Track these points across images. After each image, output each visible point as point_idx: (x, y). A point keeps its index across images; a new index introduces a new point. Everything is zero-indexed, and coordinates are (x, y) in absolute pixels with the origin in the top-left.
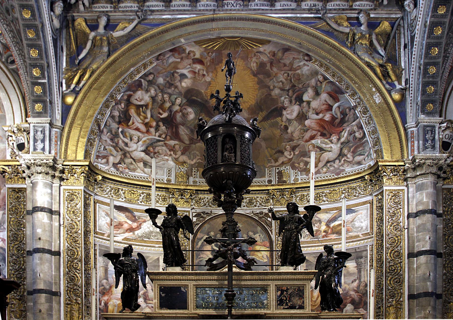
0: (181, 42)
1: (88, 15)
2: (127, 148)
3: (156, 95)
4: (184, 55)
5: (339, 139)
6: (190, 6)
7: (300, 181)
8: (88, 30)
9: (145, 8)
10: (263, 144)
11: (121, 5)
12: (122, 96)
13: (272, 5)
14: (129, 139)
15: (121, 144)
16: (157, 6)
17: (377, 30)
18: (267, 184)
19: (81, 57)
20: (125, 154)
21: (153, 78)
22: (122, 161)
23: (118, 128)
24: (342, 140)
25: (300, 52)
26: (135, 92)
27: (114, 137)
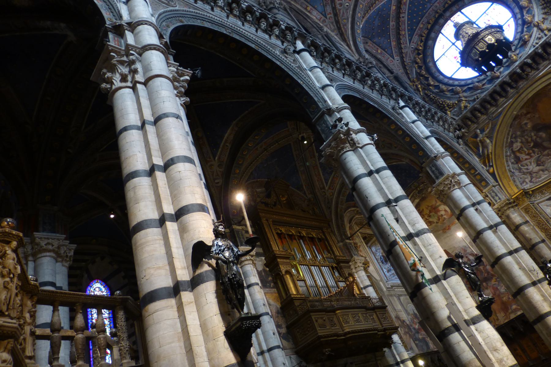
2: (529, 171)
8: (475, 140)
20: (530, 173)
26: (512, 146)
27: (520, 170)
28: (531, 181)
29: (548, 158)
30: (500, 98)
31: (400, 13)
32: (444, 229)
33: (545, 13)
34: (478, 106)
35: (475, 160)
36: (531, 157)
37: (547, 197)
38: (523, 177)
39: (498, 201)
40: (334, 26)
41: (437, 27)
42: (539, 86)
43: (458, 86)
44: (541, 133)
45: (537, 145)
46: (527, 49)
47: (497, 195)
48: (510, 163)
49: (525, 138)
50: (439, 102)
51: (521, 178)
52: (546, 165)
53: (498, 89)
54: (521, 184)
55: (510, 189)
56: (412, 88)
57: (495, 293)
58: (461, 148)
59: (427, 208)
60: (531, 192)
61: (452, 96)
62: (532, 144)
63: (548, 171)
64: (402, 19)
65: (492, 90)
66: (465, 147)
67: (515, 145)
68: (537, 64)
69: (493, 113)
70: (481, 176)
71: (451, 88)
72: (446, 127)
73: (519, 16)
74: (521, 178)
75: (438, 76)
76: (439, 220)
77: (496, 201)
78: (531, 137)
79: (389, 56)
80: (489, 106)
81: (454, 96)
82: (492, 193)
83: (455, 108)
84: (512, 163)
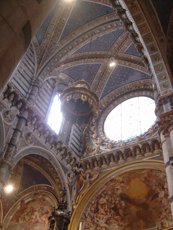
0: (113, 177)
1: (84, 175)
2: (98, 223)
4: (116, 181)
6: (116, 164)
8: (84, 180)
9: (102, 168)
12: (95, 202)
14: (99, 218)
15: (96, 221)
16: (105, 166)
19: (81, 190)
20: (97, 225)
21: (106, 192)
23: (94, 215)
25: (156, 170)
26: (100, 199)
29: (115, 222)
36: (107, 214)
38: (91, 225)
40: (41, 52)
41: (121, 99)
44: (122, 202)
45: (115, 209)
48: (89, 209)
49: (111, 199)
52: (110, 226)
59: (30, 208)
62: (113, 206)
64: (104, 82)
67: (102, 200)
68: (145, 152)
74: (88, 225)
75: (100, 128)
76: (29, 220)
78: (116, 201)
84: (91, 211)
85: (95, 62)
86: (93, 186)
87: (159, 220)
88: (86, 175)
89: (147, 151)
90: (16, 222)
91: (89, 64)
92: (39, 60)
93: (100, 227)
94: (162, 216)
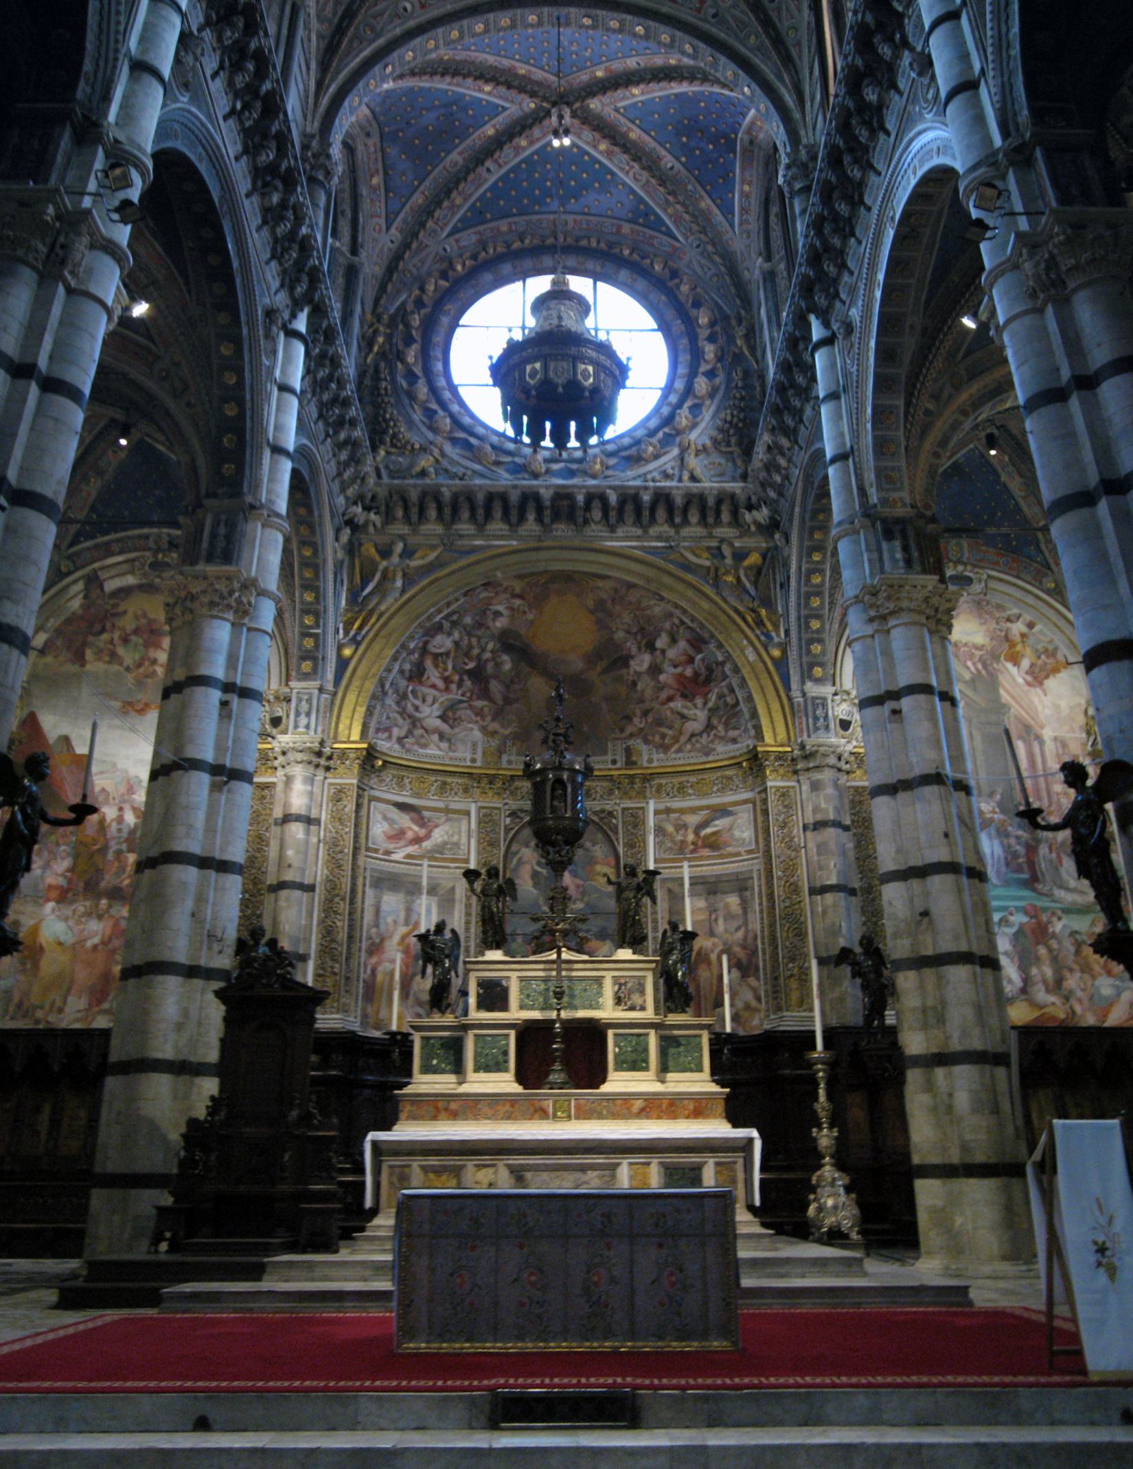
2: (417, 715)
3: (461, 639)
4: (499, 589)
5: (705, 704)
7: (655, 764)
8: (377, 558)
10: (604, 705)
11: (423, 527)
13: (613, 531)
15: (410, 708)
17: (746, 563)
18: (610, 766)
20: (415, 722)
22: (409, 733)
24: (710, 705)
25: (648, 590)
26: (433, 637)
28: (400, 740)
30: (502, 519)
31: (492, 156)
32: (130, 704)
33: (715, 442)
34: (447, 494)
35: (336, 602)
36: (447, 689)
37: (400, 799)
38: (395, 719)
39: (301, 729)
42: (582, 563)
43: (452, 416)
46: (630, 473)
47: (308, 714)
48: (397, 667)
50: (385, 412)
51: (388, 718)
52: (457, 730)
53: (514, 497)
54: (378, 730)
55: (348, 722)
56: (362, 326)
57: (110, 940)
58: (332, 549)
60: (380, 763)
61: (420, 425)
63: (450, 748)
65: (502, 490)
66: (340, 555)
67: (439, 639)
68: (621, 519)
69: (461, 536)
70: (317, 646)
71: (434, 406)
72: (347, 475)
73: (673, 399)
74: (388, 718)
76: (139, 665)
77: (296, 727)
79: (383, 212)
80: (465, 514)
81: (424, 429)
82: (304, 703)
83: (402, 454)
84: (401, 672)
85: (489, 93)
86: (422, 590)
87: (617, 739)
88: (393, 543)
89: (626, 518)
90: (73, 662)
91: (464, 95)
92: (326, 29)
93: (423, 727)
94: (629, 729)
